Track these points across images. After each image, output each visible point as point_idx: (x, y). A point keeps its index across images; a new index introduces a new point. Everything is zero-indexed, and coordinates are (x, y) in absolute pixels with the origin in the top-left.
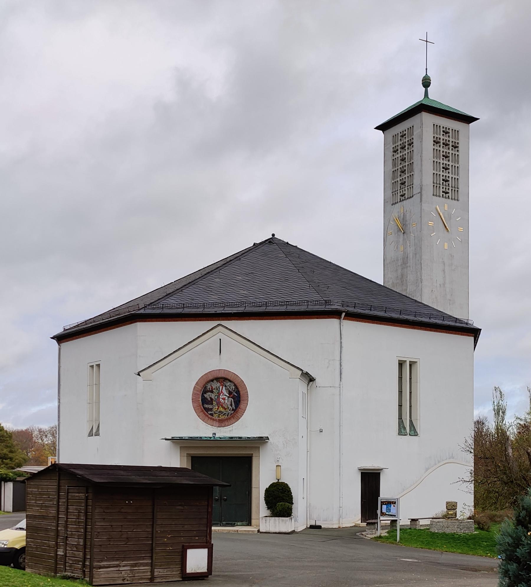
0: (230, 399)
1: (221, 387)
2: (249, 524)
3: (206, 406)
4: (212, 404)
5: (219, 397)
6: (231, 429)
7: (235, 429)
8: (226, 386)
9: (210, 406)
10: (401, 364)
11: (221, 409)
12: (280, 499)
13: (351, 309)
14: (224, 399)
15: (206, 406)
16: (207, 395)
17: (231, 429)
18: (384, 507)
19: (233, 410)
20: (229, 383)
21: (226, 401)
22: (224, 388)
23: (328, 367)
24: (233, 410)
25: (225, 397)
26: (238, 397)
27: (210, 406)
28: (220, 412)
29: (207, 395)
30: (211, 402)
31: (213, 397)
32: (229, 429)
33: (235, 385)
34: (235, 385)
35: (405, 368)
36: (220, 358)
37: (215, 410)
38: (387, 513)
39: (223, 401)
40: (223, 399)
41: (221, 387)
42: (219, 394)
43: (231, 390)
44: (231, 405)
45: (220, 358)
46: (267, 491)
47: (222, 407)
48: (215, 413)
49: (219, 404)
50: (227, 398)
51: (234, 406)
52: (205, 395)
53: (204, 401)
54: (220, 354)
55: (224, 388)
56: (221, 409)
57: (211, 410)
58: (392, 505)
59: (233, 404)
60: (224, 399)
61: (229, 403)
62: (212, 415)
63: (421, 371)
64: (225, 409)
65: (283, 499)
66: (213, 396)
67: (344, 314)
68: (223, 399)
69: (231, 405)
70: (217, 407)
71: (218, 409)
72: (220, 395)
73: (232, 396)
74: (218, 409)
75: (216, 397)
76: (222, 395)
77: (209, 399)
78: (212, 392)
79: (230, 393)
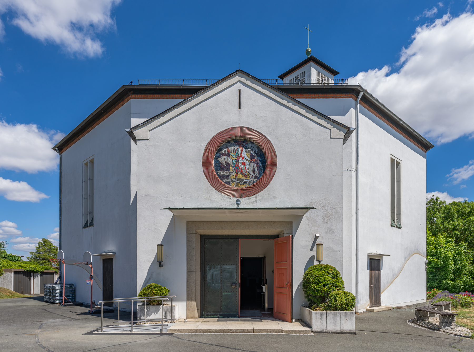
0: (252, 164)
1: (240, 150)
3: (221, 172)
4: (229, 170)
5: (237, 161)
7: (260, 200)
8: (246, 148)
9: (226, 173)
11: (240, 176)
14: (244, 164)
15: (221, 172)
16: (223, 160)
20: (250, 145)
21: (247, 167)
24: (256, 177)
25: (245, 161)
26: (264, 159)
27: (226, 173)
28: (238, 179)
29: (223, 160)
31: (230, 162)
33: (258, 147)
34: (258, 147)
36: (240, 113)
37: (232, 178)
39: (242, 166)
40: (243, 164)
41: (240, 150)
42: (238, 158)
43: (253, 153)
44: (254, 171)
45: (240, 113)
47: (241, 172)
48: (233, 181)
49: (237, 170)
50: (247, 163)
51: (257, 173)
52: (220, 160)
53: (219, 166)
54: (240, 108)
55: (244, 150)
56: (240, 176)
57: (227, 177)
59: (256, 170)
60: (244, 164)
61: (251, 169)
62: (228, 183)
64: (246, 176)
66: (230, 160)
68: (243, 164)
69: (254, 171)
70: (235, 174)
71: (236, 176)
73: (254, 160)
74: (236, 176)
76: (241, 158)
77: (225, 164)
78: (228, 155)
79: (252, 157)
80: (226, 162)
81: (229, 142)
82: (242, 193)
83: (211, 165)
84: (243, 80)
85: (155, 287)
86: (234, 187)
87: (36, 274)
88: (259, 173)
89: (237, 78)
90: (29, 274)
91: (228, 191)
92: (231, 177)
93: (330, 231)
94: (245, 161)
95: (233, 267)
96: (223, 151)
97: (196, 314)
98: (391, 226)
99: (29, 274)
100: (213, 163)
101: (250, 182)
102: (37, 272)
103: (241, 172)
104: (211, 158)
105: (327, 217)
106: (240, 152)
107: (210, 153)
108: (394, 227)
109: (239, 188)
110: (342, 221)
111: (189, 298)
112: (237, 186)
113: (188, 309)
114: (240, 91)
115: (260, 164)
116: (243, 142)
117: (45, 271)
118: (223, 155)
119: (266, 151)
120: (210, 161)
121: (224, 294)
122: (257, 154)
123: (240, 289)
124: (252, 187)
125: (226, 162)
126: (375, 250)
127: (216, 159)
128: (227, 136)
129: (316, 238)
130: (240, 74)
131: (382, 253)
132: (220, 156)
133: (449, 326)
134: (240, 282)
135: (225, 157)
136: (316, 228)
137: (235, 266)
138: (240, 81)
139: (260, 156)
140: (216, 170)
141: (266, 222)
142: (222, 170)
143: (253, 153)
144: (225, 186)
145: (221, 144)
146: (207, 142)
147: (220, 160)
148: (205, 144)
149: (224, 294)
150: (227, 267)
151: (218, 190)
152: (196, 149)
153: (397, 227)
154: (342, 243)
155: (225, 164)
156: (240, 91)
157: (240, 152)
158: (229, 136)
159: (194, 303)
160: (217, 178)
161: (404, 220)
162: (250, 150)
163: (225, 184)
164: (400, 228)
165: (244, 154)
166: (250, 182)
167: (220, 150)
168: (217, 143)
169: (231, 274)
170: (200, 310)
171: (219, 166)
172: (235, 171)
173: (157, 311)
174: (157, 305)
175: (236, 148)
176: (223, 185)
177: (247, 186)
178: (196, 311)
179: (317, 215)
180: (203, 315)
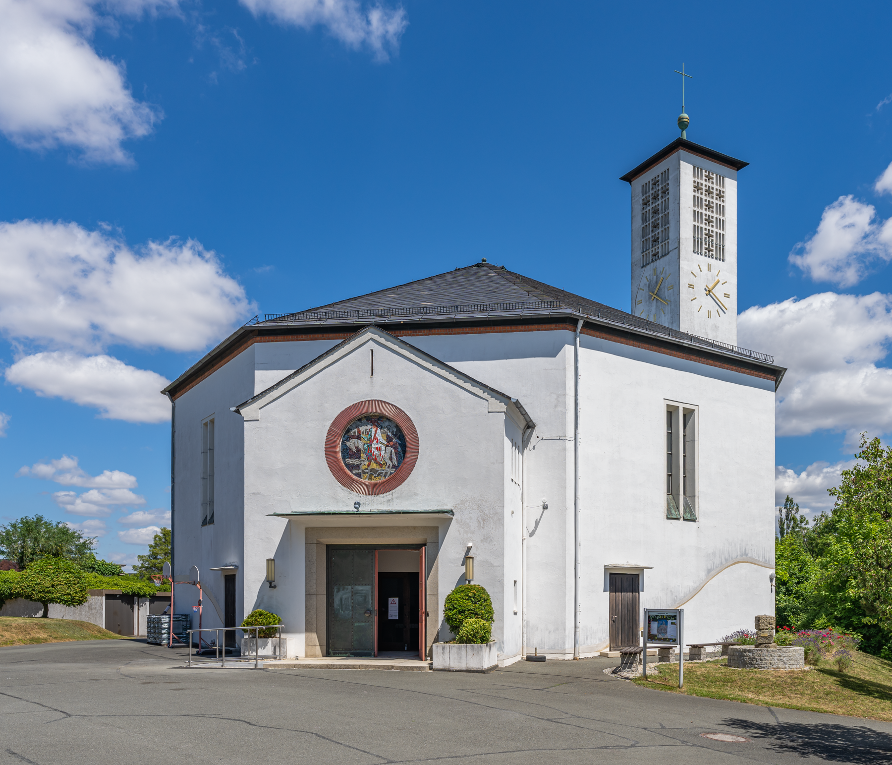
0: (389, 449)
1: (374, 430)
2: (419, 657)
3: (350, 461)
4: (359, 458)
5: (370, 446)
6: (390, 497)
7: (397, 498)
8: (381, 428)
9: (356, 462)
10: (671, 413)
11: (374, 466)
12: (472, 614)
13: (594, 318)
14: (378, 449)
15: (350, 461)
16: (352, 444)
17: (390, 497)
18: (655, 625)
19: (394, 467)
20: (387, 423)
21: (383, 453)
22: (379, 431)
23: (556, 406)
24: (394, 467)
25: (380, 445)
27: (356, 462)
28: (372, 470)
29: (352, 444)
30: (357, 454)
31: (361, 447)
32: (386, 499)
35: (679, 421)
36: (372, 382)
37: (363, 468)
38: (660, 636)
39: (376, 452)
40: (377, 448)
41: (374, 430)
42: (371, 441)
43: (390, 434)
44: (391, 459)
45: (372, 382)
46: (449, 600)
48: (364, 473)
49: (370, 457)
50: (383, 448)
51: (395, 461)
52: (348, 444)
53: (347, 452)
55: (379, 431)
56: (374, 466)
58: (669, 622)
59: (394, 457)
60: (378, 449)
61: (387, 456)
62: (359, 475)
63: (702, 423)
64: (381, 465)
65: (476, 614)
66: (360, 444)
67: (581, 323)
68: (377, 448)
69: (391, 459)
70: (367, 463)
71: (369, 465)
72: (373, 442)
73: (392, 443)
74: (369, 465)
75: (366, 446)
76: (375, 442)
77: (354, 450)
78: (359, 437)
79: (389, 440)
80: (356, 447)
81: (360, 420)
82: (375, 490)
83: (336, 453)
84: (376, 337)
85: (260, 615)
86: (367, 481)
87: (143, 599)
88: (398, 461)
89: (368, 335)
90: (131, 598)
91: (356, 486)
92: (363, 467)
93: (487, 539)
94: (380, 445)
95: (368, 588)
96: (352, 433)
97: (318, 650)
98: (668, 518)
99: (131, 598)
100: (339, 450)
101: (386, 473)
102: (144, 596)
103: (375, 460)
104: (335, 442)
105: (483, 520)
106: (373, 433)
107: (335, 436)
108: (678, 519)
109: (373, 482)
110: (503, 525)
111: (308, 630)
112: (370, 479)
113: (307, 645)
114: (372, 351)
115: (400, 449)
116: (377, 420)
117: (158, 594)
118: (352, 437)
119: (405, 432)
120: (336, 447)
121: (356, 624)
122: (395, 436)
123: (376, 618)
124: (388, 481)
125: (356, 447)
126: (623, 560)
127: (344, 444)
128: (355, 414)
129: (469, 549)
130: (372, 329)
131: (642, 565)
132: (348, 440)
133: (630, 667)
134: (376, 608)
135: (355, 440)
136: (469, 535)
137: (369, 587)
138: (371, 339)
139: (399, 438)
140: (344, 458)
141: (404, 527)
142: (350, 458)
143: (390, 434)
144: (354, 480)
145: (348, 423)
146: (331, 422)
147: (348, 444)
148: (328, 424)
149: (356, 624)
150: (360, 588)
151: (344, 485)
152: (317, 431)
153: (685, 520)
154: (503, 555)
155: (354, 450)
156: (372, 351)
157: (373, 433)
158: (358, 414)
159: (314, 635)
160: (343, 470)
161: (702, 505)
162: (386, 430)
163: (355, 477)
164: (694, 521)
165: (379, 436)
166: (386, 473)
167: (349, 431)
168: (344, 422)
169: (365, 597)
170: (325, 647)
171: (347, 452)
172: (368, 459)
173: (265, 645)
174: (265, 637)
175: (369, 427)
176: (351, 478)
177: (383, 479)
178: (318, 648)
179: (471, 518)
180: (328, 654)
